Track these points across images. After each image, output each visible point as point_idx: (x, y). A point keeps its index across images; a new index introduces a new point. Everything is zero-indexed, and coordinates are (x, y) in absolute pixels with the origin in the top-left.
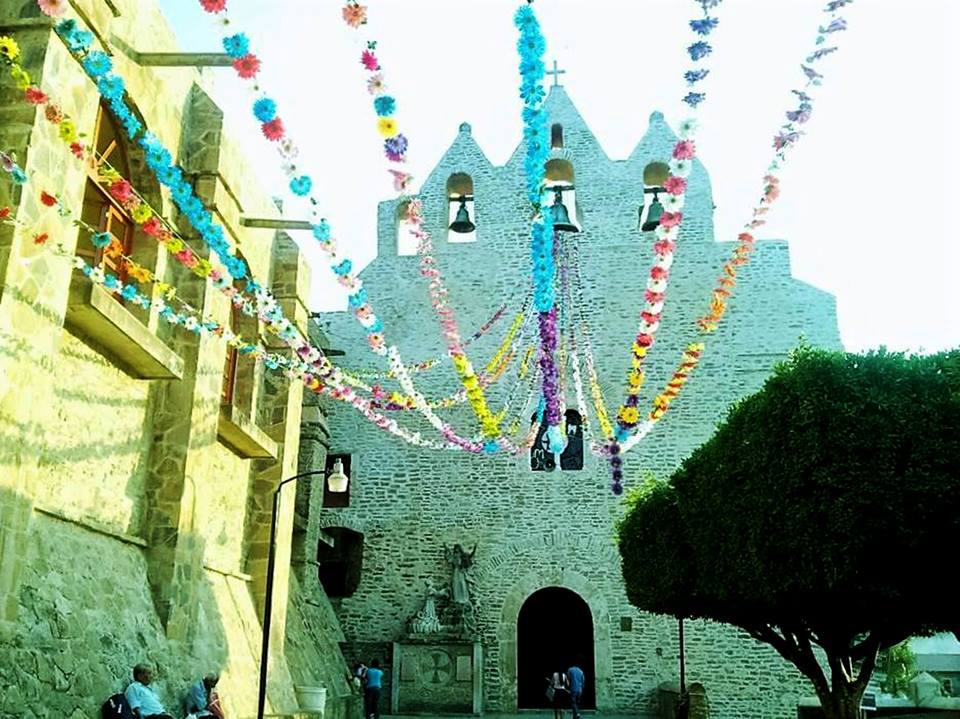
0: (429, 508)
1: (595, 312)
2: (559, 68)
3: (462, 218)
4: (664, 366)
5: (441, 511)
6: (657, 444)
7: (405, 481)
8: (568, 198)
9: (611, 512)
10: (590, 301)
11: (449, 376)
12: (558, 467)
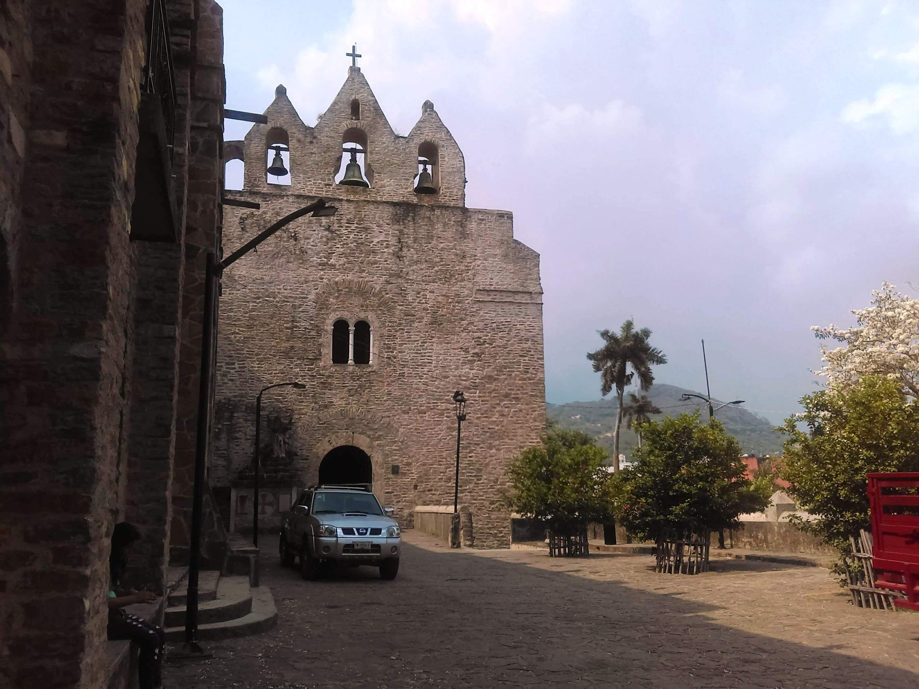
0: (254, 388)
2: (357, 52)
3: (278, 165)
7: (234, 368)
8: (360, 158)
10: (378, 242)
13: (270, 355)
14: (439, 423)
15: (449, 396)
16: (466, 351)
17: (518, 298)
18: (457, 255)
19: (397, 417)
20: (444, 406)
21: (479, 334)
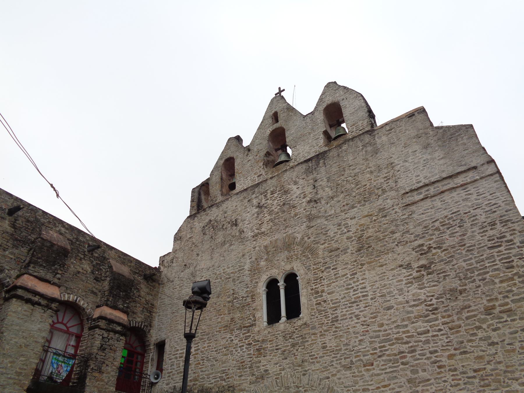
0: (204, 369)
1: (301, 202)
4: (350, 222)
5: (211, 372)
6: (352, 282)
9: (324, 348)
10: (297, 197)
11: (218, 273)
12: (283, 319)
13: (217, 332)
14: (395, 374)
15: (398, 333)
16: (408, 266)
17: (460, 180)
18: (371, 172)
19: (338, 376)
20: (397, 348)
21: (420, 242)
